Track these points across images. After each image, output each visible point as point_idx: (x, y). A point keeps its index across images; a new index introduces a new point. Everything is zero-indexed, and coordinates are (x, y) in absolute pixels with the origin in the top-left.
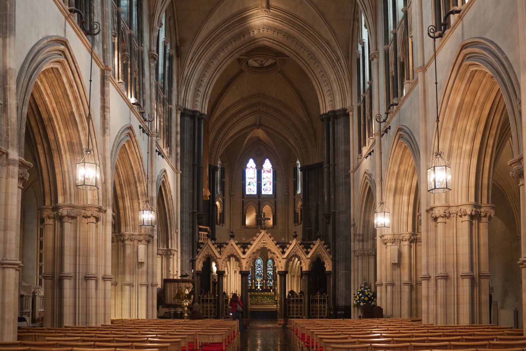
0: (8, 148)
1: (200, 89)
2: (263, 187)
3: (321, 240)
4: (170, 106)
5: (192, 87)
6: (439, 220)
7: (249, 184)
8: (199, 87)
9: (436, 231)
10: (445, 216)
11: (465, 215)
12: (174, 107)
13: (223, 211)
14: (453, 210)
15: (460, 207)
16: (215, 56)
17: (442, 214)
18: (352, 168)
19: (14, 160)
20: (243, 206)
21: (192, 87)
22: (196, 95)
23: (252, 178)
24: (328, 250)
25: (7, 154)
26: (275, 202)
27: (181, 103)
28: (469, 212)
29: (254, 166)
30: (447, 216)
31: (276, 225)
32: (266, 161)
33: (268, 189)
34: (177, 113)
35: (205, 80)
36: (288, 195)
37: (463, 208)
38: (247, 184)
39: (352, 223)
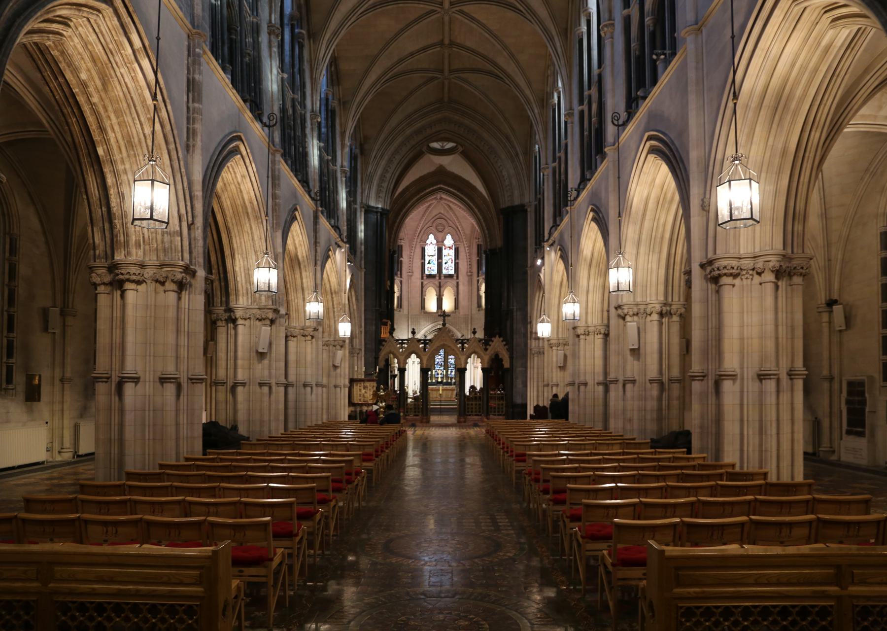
0: (279, 306)
1: (383, 185)
2: (444, 265)
3: (500, 337)
4: (355, 206)
5: (375, 184)
6: (582, 337)
7: (429, 263)
8: (382, 183)
9: (579, 345)
10: (585, 334)
11: (600, 334)
12: (358, 206)
13: (401, 295)
14: (591, 329)
15: (597, 327)
16: (396, 152)
17: (583, 333)
18: (529, 266)
19: (283, 315)
20: (422, 287)
21: (375, 184)
22: (378, 192)
23: (433, 256)
24: (506, 347)
25: (279, 311)
26: (458, 283)
27: (364, 201)
28: (603, 332)
29: (435, 242)
30: (587, 334)
31: (458, 309)
32: (447, 237)
33: (449, 268)
34: (361, 211)
35: (388, 176)
36: (471, 275)
37: (599, 328)
38: (427, 262)
39: (529, 320)
